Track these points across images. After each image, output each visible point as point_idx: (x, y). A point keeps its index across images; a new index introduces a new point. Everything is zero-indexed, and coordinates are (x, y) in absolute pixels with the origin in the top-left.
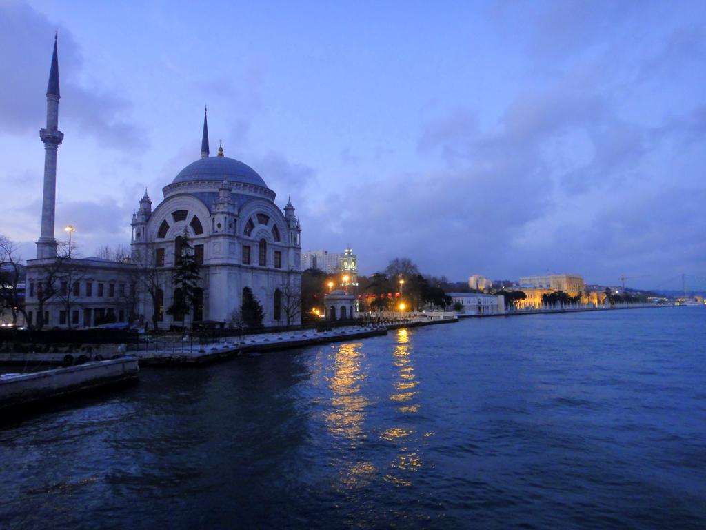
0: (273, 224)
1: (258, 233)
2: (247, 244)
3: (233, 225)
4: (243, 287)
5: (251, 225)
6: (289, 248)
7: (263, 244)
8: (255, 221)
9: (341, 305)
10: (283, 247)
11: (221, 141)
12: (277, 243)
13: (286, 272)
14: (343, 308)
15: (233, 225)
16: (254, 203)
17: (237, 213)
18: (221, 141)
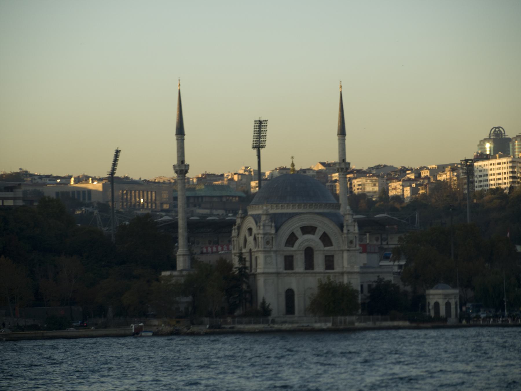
0: (321, 233)
1: (302, 242)
2: (288, 254)
3: (271, 241)
4: (287, 287)
5: (292, 239)
6: (343, 251)
7: (309, 253)
8: (298, 233)
9: (434, 301)
10: (335, 251)
11: (292, 158)
12: (327, 248)
13: (339, 273)
14: (437, 305)
15: (271, 241)
16: (296, 219)
17: (273, 231)
18: (292, 158)
